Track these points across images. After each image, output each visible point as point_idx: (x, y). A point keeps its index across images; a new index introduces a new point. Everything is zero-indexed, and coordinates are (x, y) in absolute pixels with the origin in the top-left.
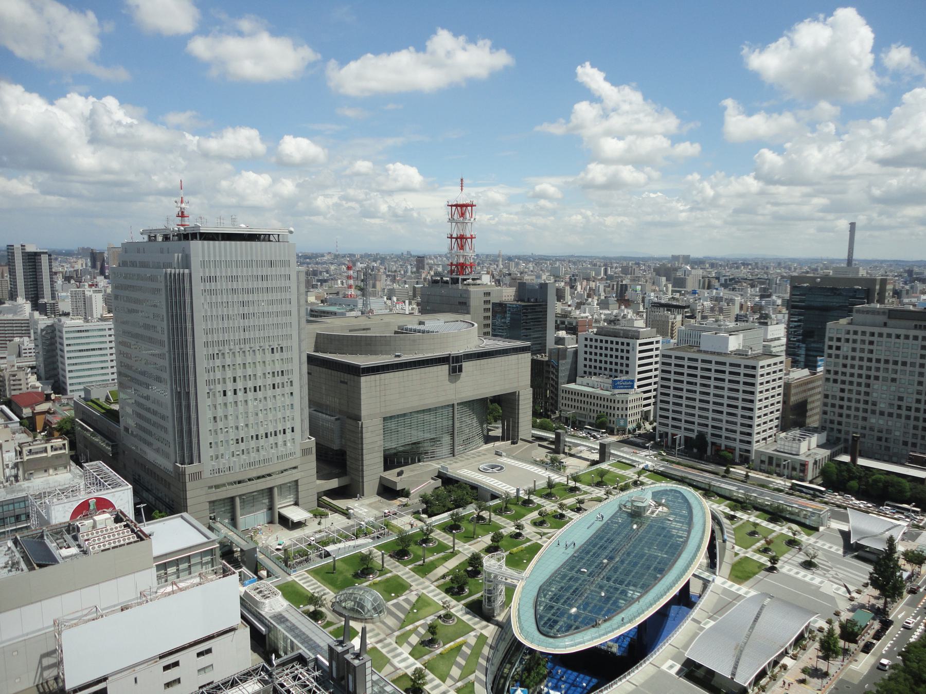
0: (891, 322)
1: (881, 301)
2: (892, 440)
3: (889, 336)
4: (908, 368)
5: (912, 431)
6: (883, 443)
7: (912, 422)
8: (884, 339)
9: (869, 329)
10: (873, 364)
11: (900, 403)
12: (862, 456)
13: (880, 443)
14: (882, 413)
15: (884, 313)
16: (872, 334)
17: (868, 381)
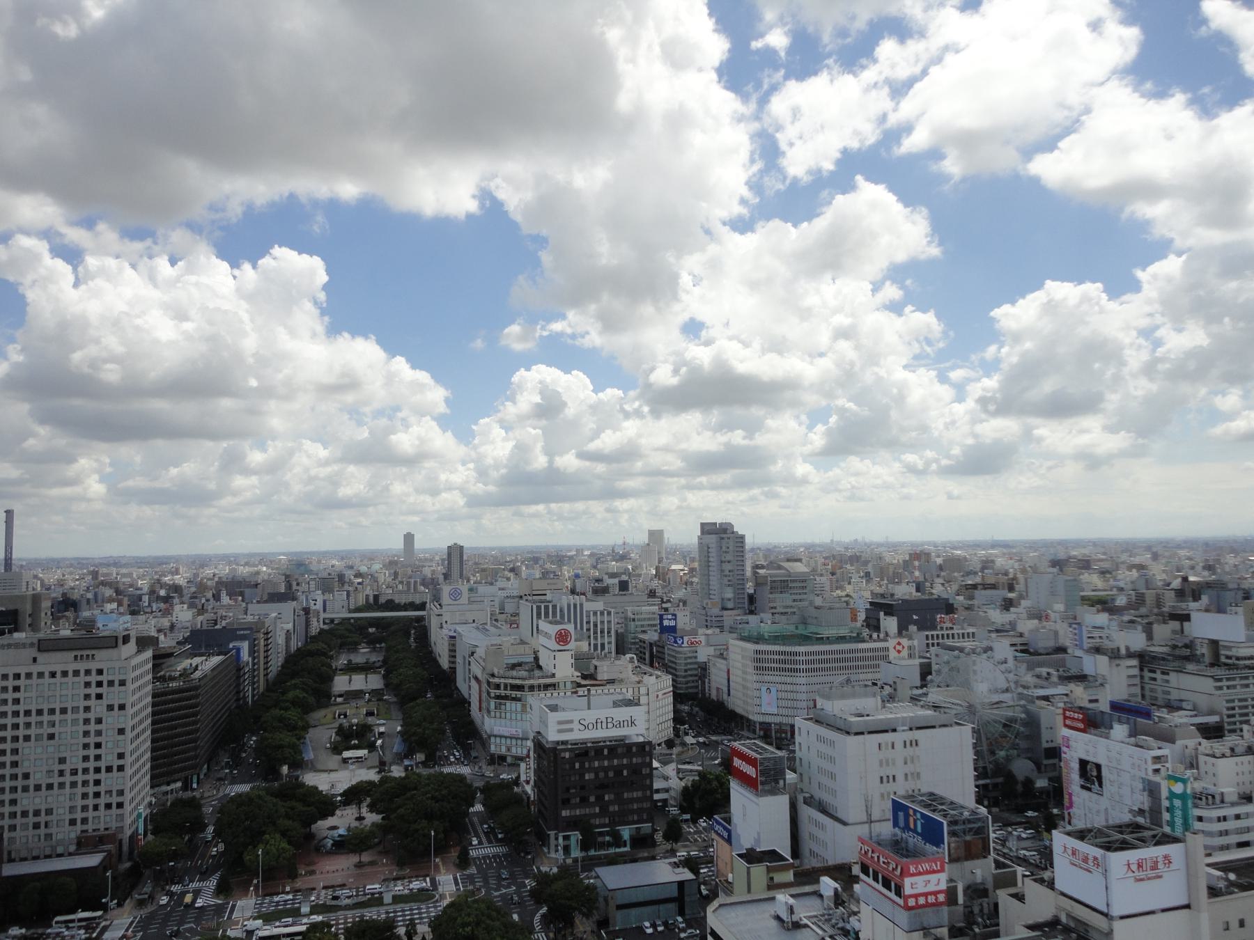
0: (42, 657)
1: (34, 627)
2: (55, 822)
3: (41, 675)
4: (69, 716)
5: (80, 803)
6: (43, 831)
7: (80, 790)
8: (35, 680)
9: (11, 671)
10: (21, 720)
11: (62, 767)
12: (11, 860)
13: (37, 832)
14: (38, 788)
15: (32, 645)
16: (17, 676)
17: (15, 745)
